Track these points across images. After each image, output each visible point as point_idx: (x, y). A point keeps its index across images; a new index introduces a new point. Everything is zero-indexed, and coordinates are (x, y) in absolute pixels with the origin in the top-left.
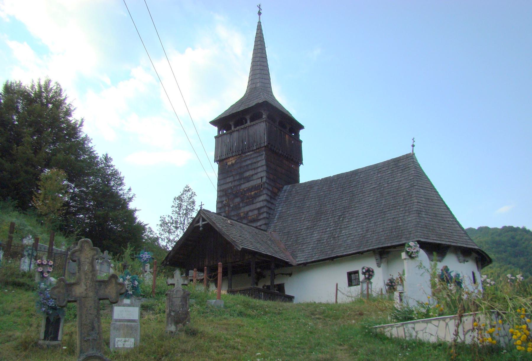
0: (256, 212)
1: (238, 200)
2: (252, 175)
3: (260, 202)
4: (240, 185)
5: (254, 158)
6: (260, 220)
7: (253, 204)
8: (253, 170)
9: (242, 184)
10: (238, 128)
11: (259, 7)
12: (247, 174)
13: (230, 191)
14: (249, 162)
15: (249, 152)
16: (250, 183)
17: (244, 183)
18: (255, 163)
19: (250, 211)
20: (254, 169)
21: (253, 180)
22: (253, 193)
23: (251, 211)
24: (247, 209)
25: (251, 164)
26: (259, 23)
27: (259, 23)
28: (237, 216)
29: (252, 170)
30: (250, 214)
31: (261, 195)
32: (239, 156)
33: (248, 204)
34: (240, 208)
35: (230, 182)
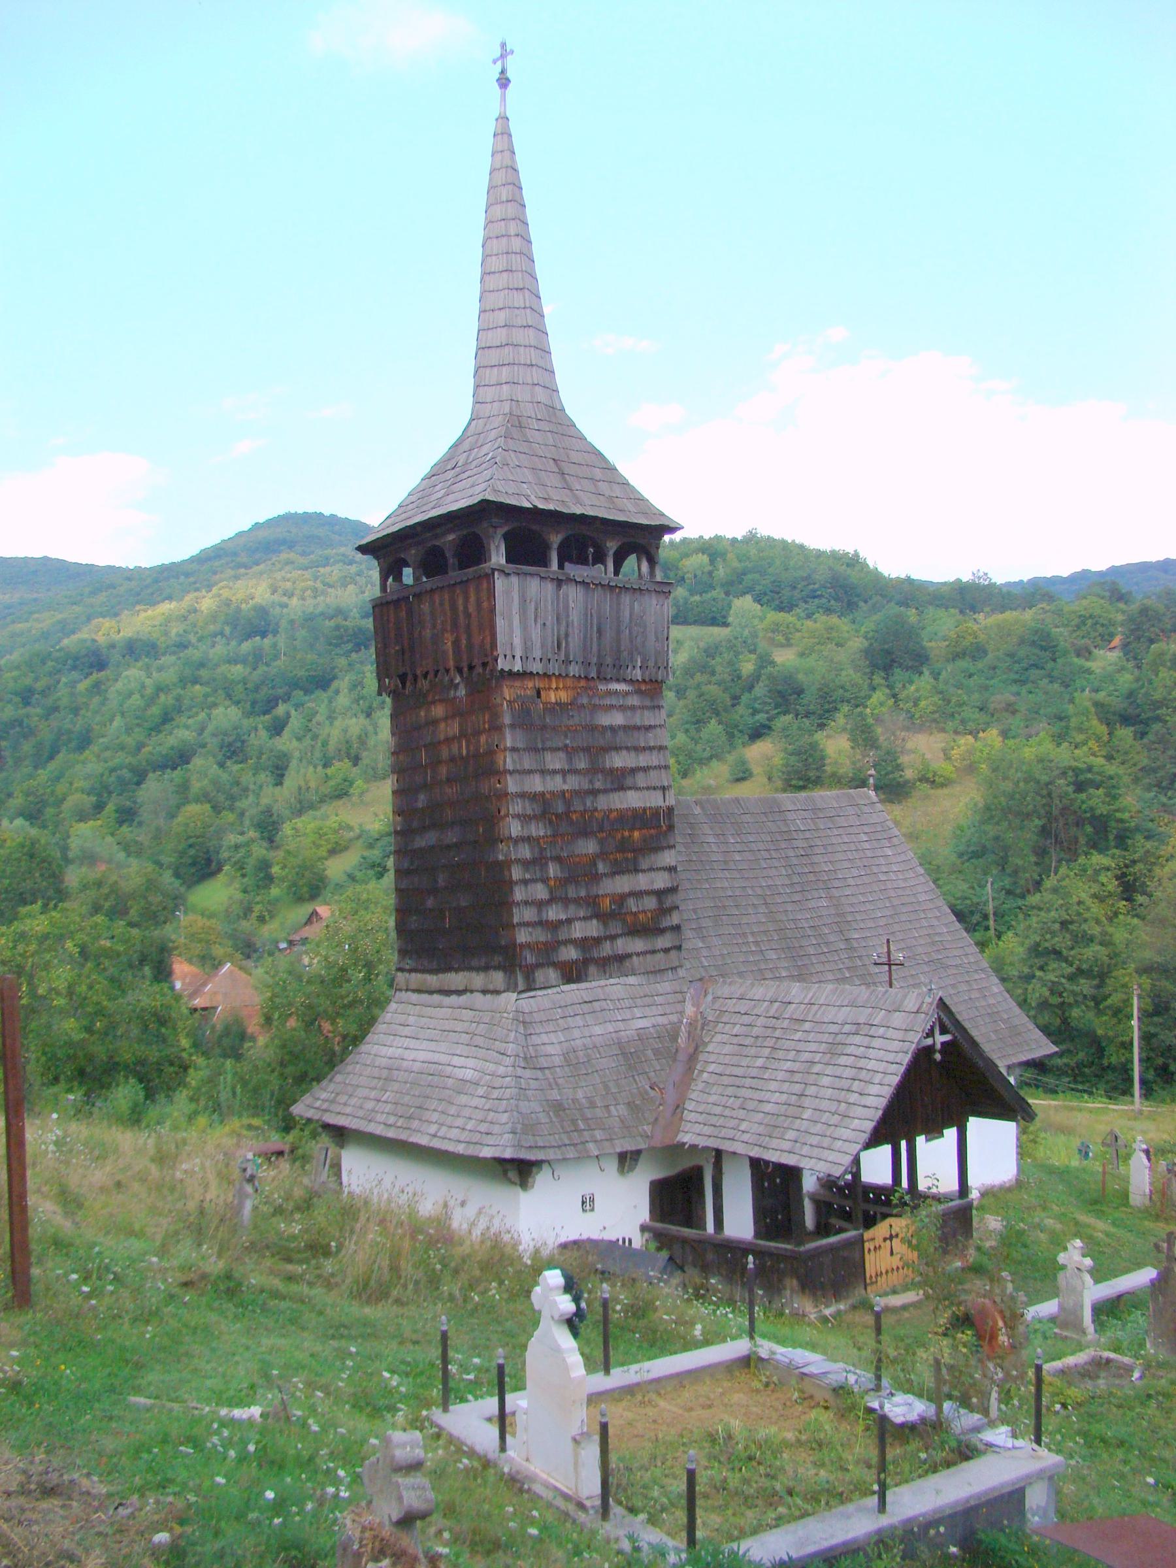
0: (650, 903)
1: (589, 847)
2: (634, 771)
3: (664, 869)
4: (594, 793)
5: (633, 708)
6: (662, 931)
7: (637, 871)
8: (633, 754)
9: (599, 791)
10: (572, 570)
11: (505, 52)
12: (618, 760)
13: (561, 809)
14: (618, 719)
15: (618, 680)
16: (630, 793)
17: (605, 791)
18: (637, 728)
19: (632, 894)
20: (637, 749)
21: (637, 789)
22: (636, 834)
23: (638, 894)
24: (622, 884)
25: (625, 728)
26: (503, 119)
27: (503, 119)
28: (588, 904)
29: (627, 748)
30: (632, 905)
31: (662, 849)
32: (583, 683)
33: (618, 870)
34: (596, 878)
35: (555, 772)
